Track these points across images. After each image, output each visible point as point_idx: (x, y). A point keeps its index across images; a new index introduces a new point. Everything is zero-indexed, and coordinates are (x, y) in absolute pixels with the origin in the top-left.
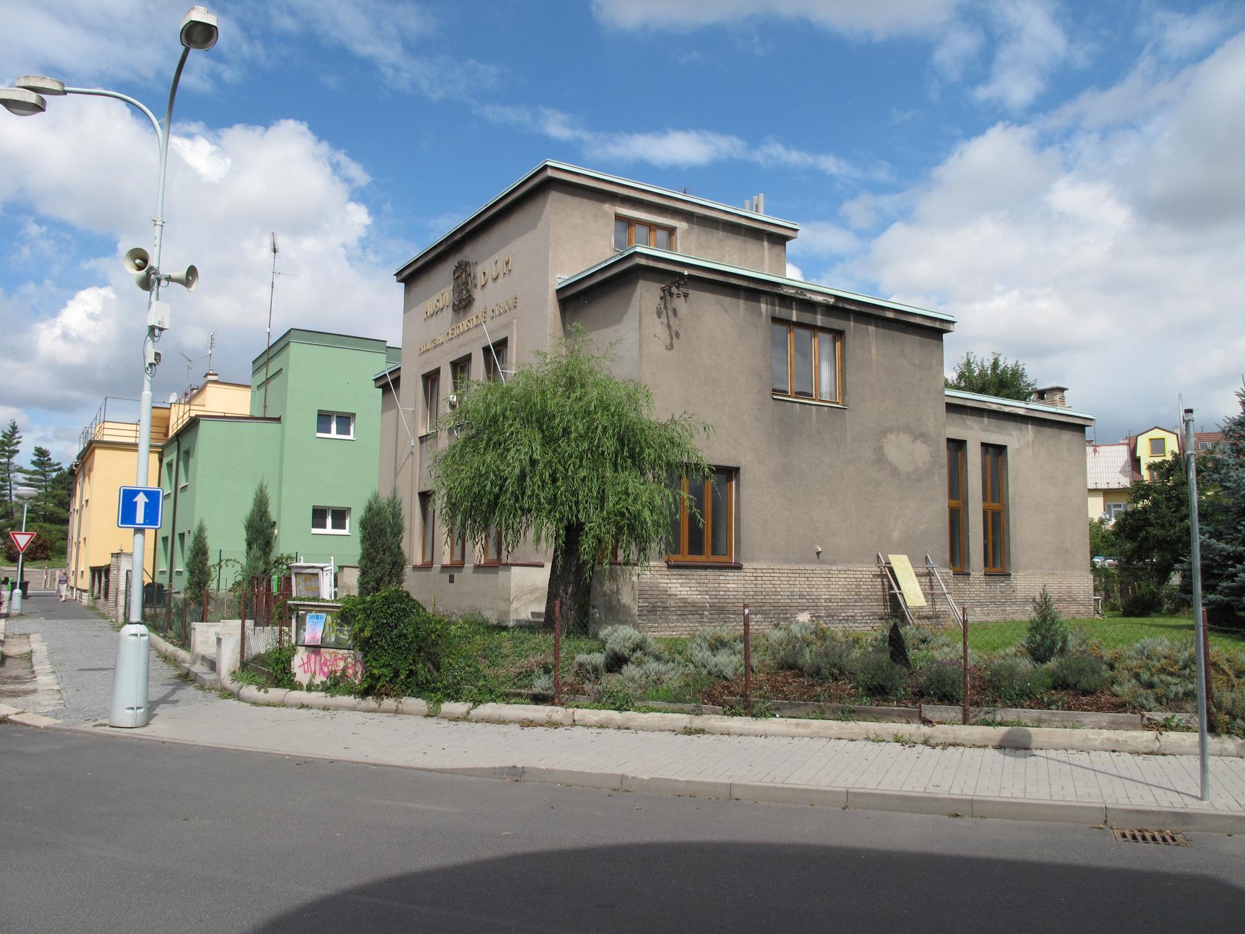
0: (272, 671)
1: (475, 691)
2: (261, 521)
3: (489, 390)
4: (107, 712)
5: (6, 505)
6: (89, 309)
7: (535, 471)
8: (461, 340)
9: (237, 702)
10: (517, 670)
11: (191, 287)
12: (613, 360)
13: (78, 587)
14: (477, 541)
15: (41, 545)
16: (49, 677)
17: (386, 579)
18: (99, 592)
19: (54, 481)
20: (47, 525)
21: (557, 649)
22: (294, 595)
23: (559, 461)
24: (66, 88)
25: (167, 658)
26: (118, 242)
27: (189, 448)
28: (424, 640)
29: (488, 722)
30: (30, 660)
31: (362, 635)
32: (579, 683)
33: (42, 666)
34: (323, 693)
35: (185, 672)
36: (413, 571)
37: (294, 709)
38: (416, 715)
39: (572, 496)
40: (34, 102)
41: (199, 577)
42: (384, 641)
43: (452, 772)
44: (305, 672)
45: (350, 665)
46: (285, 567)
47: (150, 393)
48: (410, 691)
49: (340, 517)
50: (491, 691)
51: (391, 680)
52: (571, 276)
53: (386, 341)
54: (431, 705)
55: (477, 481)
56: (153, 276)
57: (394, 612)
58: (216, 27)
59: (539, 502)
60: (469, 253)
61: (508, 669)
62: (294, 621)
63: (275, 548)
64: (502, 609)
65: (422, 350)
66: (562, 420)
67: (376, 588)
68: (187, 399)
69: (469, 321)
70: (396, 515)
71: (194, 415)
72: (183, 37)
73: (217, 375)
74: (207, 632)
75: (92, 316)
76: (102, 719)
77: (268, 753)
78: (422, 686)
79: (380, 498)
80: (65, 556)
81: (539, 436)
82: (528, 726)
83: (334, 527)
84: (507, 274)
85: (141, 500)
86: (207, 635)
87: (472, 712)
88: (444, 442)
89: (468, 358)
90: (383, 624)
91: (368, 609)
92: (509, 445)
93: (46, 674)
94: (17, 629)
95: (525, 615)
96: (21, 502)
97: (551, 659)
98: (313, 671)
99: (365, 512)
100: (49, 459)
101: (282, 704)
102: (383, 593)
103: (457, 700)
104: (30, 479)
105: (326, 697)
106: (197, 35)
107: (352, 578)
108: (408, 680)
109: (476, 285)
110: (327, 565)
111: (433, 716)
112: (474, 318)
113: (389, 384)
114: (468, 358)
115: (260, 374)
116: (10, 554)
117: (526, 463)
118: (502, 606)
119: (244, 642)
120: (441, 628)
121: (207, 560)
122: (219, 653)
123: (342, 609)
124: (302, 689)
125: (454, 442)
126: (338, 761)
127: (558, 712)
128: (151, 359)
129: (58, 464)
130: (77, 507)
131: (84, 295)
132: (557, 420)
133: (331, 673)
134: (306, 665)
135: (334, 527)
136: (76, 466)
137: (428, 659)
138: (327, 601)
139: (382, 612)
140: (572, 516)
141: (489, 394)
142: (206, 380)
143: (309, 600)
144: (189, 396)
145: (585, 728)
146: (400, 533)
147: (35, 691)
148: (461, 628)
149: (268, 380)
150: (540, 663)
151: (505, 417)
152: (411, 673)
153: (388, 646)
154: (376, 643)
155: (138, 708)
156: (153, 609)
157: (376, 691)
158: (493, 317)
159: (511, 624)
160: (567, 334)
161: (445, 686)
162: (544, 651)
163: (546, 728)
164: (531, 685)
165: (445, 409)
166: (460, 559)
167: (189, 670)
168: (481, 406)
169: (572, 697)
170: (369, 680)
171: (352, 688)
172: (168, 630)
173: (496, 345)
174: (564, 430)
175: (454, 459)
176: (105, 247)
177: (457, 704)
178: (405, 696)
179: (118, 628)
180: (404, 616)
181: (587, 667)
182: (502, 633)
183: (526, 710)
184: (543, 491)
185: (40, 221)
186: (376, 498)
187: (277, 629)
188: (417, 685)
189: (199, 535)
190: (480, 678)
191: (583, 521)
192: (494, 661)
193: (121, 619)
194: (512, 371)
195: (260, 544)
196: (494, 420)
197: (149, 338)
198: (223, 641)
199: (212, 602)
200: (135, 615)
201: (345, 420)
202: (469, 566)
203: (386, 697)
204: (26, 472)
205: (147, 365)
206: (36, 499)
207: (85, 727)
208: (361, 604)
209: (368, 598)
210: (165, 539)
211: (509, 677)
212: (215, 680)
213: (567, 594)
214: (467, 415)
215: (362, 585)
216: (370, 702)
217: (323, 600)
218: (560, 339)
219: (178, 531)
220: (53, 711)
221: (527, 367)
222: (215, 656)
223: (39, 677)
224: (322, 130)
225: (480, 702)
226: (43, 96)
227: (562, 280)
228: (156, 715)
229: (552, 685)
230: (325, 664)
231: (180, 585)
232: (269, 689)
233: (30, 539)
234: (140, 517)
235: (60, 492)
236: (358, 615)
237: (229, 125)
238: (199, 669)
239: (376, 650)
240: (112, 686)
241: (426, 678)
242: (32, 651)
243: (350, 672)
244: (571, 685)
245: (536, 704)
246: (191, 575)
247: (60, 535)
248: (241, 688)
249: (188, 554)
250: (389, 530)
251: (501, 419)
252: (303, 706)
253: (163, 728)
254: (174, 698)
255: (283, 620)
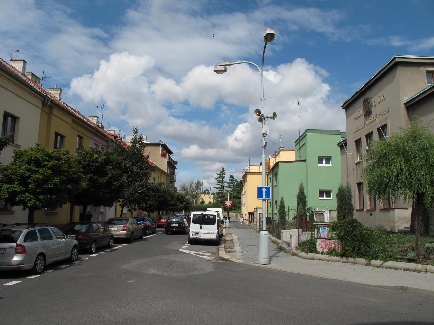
0: (309, 247)
1: (384, 256)
2: (302, 195)
3: (382, 143)
4: (257, 259)
5: (223, 193)
6: (242, 130)
7: (402, 173)
8: (368, 127)
9: (298, 257)
10: (401, 249)
11: (275, 119)
12: (432, 127)
13: (245, 219)
14: (381, 200)
15: (233, 206)
16: (239, 247)
17: (347, 215)
18: (251, 220)
19: (236, 185)
20: (234, 199)
21: (417, 241)
22: (315, 221)
23: (412, 168)
24: (232, 63)
25: (274, 242)
26: (249, 108)
27: (276, 172)
28: (363, 237)
29: (390, 268)
30: (233, 241)
31: (340, 235)
32: (427, 255)
33: (236, 244)
34: (327, 255)
35: (280, 247)
36: (356, 212)
37: (317, 261)
38: (362, 264)
39: (419, 182)
40: (224, 69)
41: (282, 215)
42: (348, 237)
43: (378, 286)
44: (321, 248)
45: (336, 246)
46: (310, 211)
47: (264, 155)
48: (359, 255)
49: (328, 193)
50: (390, 257)
51: (352, 251)
52: (410, 97)
53: (340, 130)
54: (367, 261)
55: (380, 178)
56: (262, 117)
57: (352, 226)
58: (274, 34)
59: (405, 185)
60: (368, 95)
61: (397, 248)
62: (316, 230)
63: (307, 205)
64: (392, 225)
65: (354, 132)
66: (412, 153)
67: (343, 218)
68: (274, 156)
69: (371, 119)
70: (349, 192)
71: (277, 162)
72: (265, 39)
73: (283, 147)
74: (286, 233)
75: (243, 133)
76: (256, 261)
77: (309, 275)
78: (364, 254)
79: (343, 185)
80: (240, 209)
81: (403, 159)
82: (407, 271)
83: (326, 197)
84: (384, 100)
85: (264, 190)
86: (286, 234)
87: (383, 264)
88: (365, 165)
89: (371, 133)
90: (348, 231)
91: (342, 226)
92: (391, 163)
93: (238, 246)
94: (228, 232)
95: (402, 228)
96: (227, 192)
97: (414, 245)
98: (323, 247)
99: (338, 191)
100: (234, 179)
101: (313, 259)
102: (347, 220)
103: (377, 260)
104: (229, 185)
105: (328, 257)
106: (269, 38)
107: (335, 215)
108: (358, 252)
109: (372, 106)
110: (326, 210)
111: (368, 265)
112: (373, 118)
113: (343, 145)
114: (371, 133)
115: (298, 146)
116: (225, 208)
117: (399, 170)
118: (392, 224)
119: (299, 237)
120: (370, 233)
121: (285, 209)
122: (291, 241)
123: (333, 226)
124: (320, 254)
125: (369, 164)
126: (334, 280)
127: (419, 266)
128: (264, 144)
129: (237, 180)
130: (243, 193)
131: (240, 126)
132: (410, 153)
133: (330, 248)
134: (321, 245)
135: (326, 197)
136: (242, 180)
137: (365, 244)
138: (327, 223)
139: (347, 227)
140: (419, 189)
141: (382, 145)
142: (280, 150)
143: (321, 222)
144: (275, 155)
145: (432, 273)
146: (351, 198)
147: (235, 251)
148: (377, 233)
149: (300, 148)
150: (410, 247)
151: (389, 154)
152: (359, 249)
153: (350, 239)
154: (346, 238)
155: (266, 258)
156: (268, 226)
157: (346, 255)
158: (380, 117)
159: (396, 231)
160: (411, 119)
161: (372, 254)
162: (412, 242)
163: (415, 272)
164: (407, 255)
165: (364, 153)
166: (374, 207)
167: (281, 246)
168: (379, 150)
169: (425, 260)
170: (343, 251)
171: (337, 254)
172: (274, 233)
173: (382, 127)
174: (414, 156)
175: (370, 170)
176: (245, 110)
177: (377, 261)
178: (357, 257)
179: (259, 232)
180: (356, 228)
181: (431, 248)
182: (393, 235)
183: (405, 265)
184: (406, 180)
185: (226, 105)
186: (342, 186)
187: (310, 232)
188: (362, 253)
189: (282, 201)
190: (386, 252)
191: (424, 191)
192: (391, 245)
193: (258, 229)
194: (389, 136)
195: (302, 203)
196: (385, 155)
197: (263, 138)
198: (292, 236)
199: (287, 223)
200: (264, 227)
201: (328, 159)
202: (378, 209)
203: (350, 257)
204: (228, 183)
205: (263, 146)
206: (231, 191)
207: (250, 264)
208: (339, 224)
209: (342, 222)
210: (271, 203)
211: (398, 252)
212: (290, 250)
213: (419, 220)
214: (374, 154)
215: (338, 217)
216: (344, 259)
217: (326, 223)
218: (409, 122)
219: (274, 200)
220: (241, 258)
221: (396, 134)
222: (290, 242)
223: (236, 247)
224: (310, 60)
225: (387, 261)
226: (226, 67)
227: (406, 99)
228: (272, 261)
229: (416, 255)
230: (327, 245)
231: (276, 218)
232: (308, 253)
233: (230, 204)
234: (264, 196)
235: (238, 189)
236: (338, 228)
237: (279, 64)
238: (284, 246)
239: (346, 240)
240: (258, 251)
241: (365, 251)
242: (233, 239)
243: (336, 248)
244: (424, 255)
245: (410, 262)
246: (280, 214)
247: (238, 202)
248: (299, 252)
249: (278, 208)
250: (347, 197)
251: (388, 154)
252: (320, 260)
253: (274, 265)
254: (277, 255)
255: (312, 229)
